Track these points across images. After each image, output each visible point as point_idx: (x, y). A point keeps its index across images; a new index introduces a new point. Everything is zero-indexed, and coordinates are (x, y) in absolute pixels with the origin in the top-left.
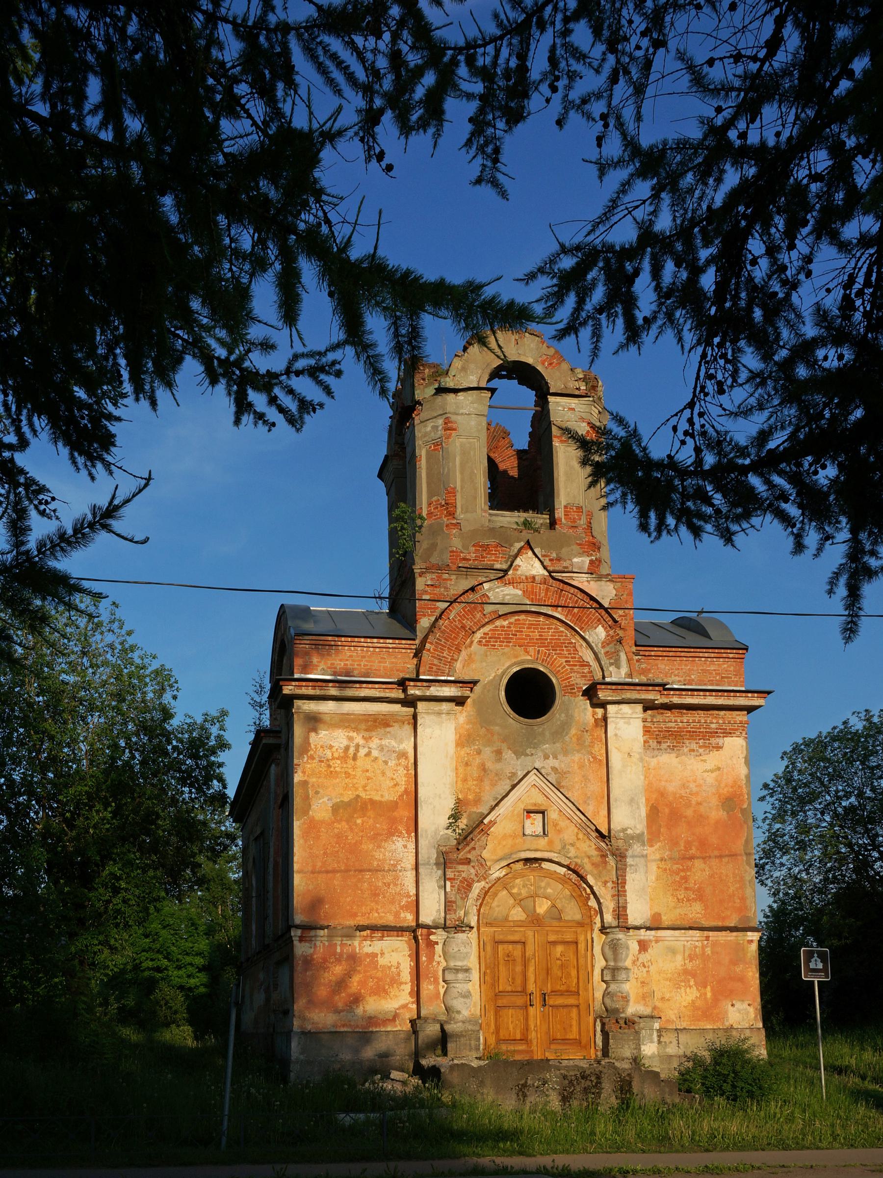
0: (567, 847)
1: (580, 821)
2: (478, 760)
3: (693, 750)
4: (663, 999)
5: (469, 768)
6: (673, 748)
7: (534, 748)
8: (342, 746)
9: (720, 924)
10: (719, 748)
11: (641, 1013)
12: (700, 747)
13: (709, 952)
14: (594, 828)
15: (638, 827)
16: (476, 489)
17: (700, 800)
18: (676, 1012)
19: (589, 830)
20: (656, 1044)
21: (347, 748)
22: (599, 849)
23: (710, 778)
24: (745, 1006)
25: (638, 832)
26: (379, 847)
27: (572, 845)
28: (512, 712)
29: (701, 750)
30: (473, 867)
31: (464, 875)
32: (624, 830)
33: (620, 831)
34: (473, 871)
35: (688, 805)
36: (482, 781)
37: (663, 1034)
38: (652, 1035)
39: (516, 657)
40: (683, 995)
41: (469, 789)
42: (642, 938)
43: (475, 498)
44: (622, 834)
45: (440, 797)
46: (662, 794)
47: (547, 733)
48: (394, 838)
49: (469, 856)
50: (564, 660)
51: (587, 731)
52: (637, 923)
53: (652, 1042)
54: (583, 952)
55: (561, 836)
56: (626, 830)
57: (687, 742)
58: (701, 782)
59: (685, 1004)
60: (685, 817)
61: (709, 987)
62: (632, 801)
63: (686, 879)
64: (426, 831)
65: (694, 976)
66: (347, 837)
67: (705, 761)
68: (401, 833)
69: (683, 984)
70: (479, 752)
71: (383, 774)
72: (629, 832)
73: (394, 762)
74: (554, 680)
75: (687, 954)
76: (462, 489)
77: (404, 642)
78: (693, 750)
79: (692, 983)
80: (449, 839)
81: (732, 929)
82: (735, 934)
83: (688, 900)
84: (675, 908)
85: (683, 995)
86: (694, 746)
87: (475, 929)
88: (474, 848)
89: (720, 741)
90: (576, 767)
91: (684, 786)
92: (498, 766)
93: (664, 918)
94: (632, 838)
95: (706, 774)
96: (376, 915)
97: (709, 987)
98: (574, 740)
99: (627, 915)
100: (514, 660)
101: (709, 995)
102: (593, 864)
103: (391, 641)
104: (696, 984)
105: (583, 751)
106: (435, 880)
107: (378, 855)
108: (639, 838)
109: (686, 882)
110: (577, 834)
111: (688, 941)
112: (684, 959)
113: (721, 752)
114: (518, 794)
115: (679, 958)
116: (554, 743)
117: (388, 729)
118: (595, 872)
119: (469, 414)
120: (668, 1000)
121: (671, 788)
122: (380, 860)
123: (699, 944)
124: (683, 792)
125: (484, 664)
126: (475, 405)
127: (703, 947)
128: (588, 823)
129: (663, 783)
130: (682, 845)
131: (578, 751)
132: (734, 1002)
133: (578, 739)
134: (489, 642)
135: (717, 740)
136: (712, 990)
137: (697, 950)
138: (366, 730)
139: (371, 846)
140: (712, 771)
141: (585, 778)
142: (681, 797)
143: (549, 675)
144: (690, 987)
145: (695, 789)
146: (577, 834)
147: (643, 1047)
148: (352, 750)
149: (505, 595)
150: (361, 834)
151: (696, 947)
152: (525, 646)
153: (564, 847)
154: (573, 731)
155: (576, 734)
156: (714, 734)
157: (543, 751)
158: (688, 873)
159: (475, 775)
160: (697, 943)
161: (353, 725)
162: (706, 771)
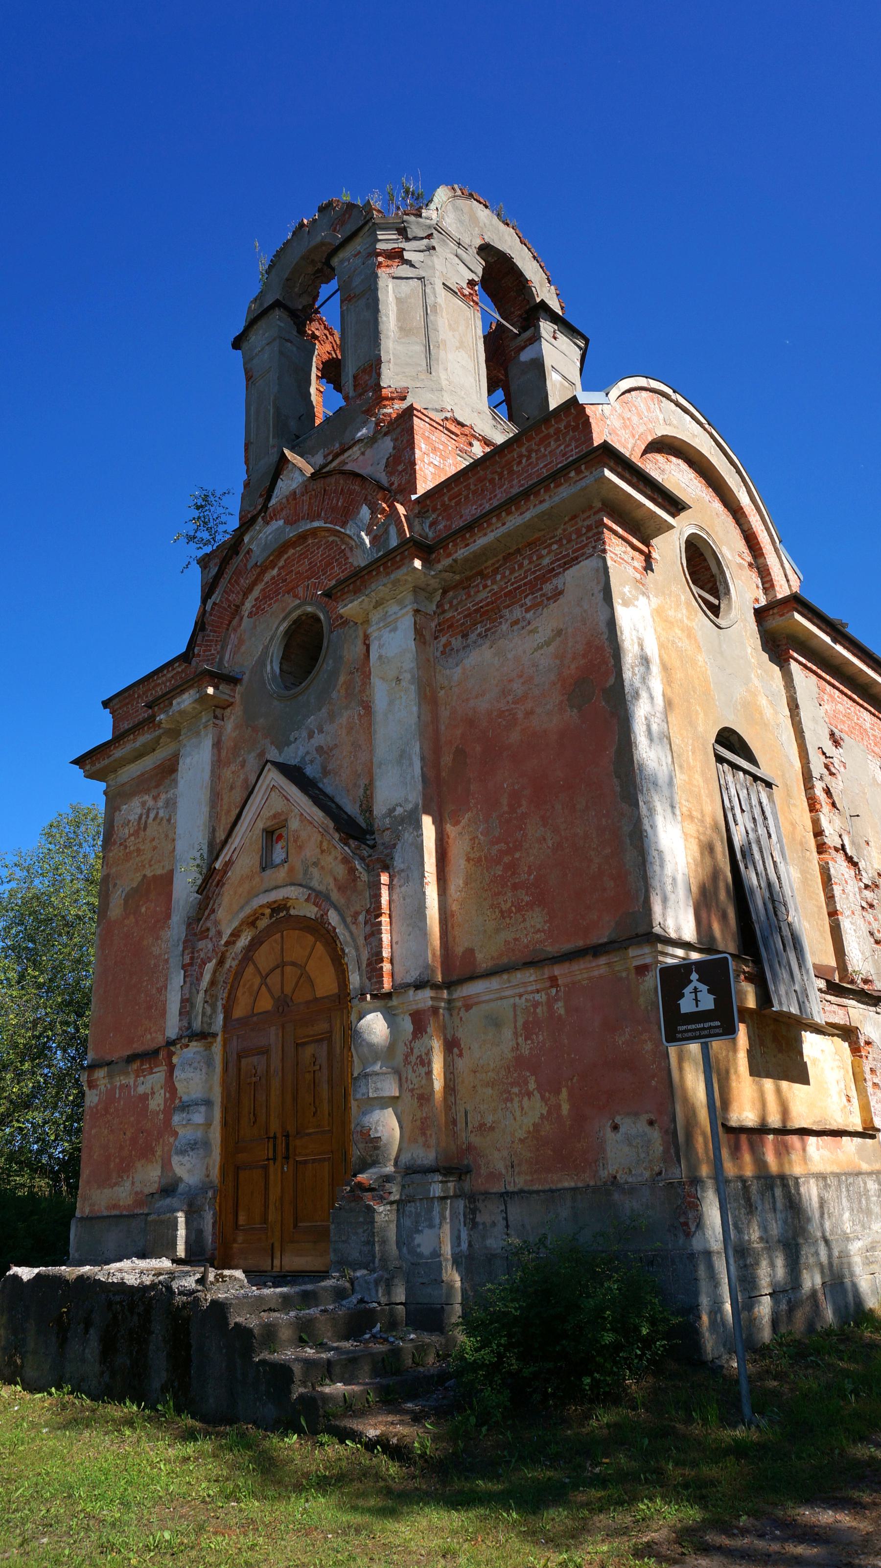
4: (482, 1126)
9: (580, 943)
10: (558, 594)
13: (562, 1011)
18: (505, 1153)
24: (641, 1126)
27: (315, 864)
29: (529, 616)
37: (480, 1205)
40: (518, 1114)
42: (414, 1007)
54: (338, 1051)
57: (506, 612)
59: (520, 1134)
61: (564, 1093)
62: (403, 756)
63: (512, 867)
69: (516, 1090)
72: (399, 811)
75: (520, 1023)
79: (532, 1086)
81: (596, 951)
82: (603, 960)
83: (519, 909)
84: (497, 931)
85: (518, 1114)
86: (518, 612)
87: (219, 1039)
89: (558, 582)
91: (504, 693)
93: (479, 956)
96: (149, 1036)
97: (564, 1093)
101: (565, 1108)
104: (539, 1088)
107: (156, 951)
109: (513, 874)
110: (321, 842)
111: (520, 996)
112: (515, 1034)
113: (562, 600)
114: (254, 809)
115: (507, 1033)
120: (492, 1129)
123: (541, 997)
132: (618, 1120)
136: (571, 1095)
137: (539, 1010)
140: (547, 644)
144: (529, 1094)
146: (321, 842)
151: (536, 1005)
156: (551, 573)
160: (537, 997)
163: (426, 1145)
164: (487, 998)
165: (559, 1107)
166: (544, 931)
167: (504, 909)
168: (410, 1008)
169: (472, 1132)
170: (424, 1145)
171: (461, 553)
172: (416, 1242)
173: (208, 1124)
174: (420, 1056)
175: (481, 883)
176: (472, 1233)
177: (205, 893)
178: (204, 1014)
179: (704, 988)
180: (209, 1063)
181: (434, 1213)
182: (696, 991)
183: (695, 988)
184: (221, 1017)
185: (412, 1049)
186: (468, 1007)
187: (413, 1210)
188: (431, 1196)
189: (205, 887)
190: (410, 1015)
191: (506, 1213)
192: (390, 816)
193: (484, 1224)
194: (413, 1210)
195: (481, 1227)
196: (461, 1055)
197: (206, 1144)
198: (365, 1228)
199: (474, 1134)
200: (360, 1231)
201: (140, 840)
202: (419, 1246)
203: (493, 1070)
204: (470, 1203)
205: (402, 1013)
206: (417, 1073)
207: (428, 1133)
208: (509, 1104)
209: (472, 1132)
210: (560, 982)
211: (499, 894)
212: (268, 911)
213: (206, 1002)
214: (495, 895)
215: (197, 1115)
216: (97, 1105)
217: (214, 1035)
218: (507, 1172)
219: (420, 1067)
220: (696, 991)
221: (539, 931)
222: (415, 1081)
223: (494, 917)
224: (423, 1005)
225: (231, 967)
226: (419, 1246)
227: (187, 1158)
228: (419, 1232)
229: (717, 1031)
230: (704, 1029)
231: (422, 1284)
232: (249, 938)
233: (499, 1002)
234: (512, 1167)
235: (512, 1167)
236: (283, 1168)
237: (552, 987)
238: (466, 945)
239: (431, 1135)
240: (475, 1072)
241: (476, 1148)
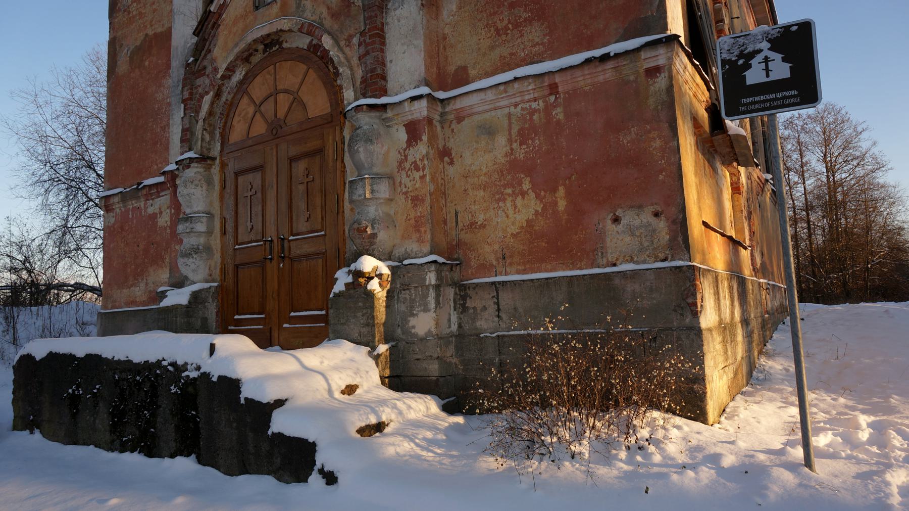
4: (473, 224)
13: (561, 116)
18: (496, 247)
20: (432, 314)
24: (646, 217)
38: (425, 296)
40: (511, 212)
42: (410, 118)
59: (514, 229)
61: (561, 191)
65: (529, 170)
69: (509, 191)
75: (515, 131)
79: (526, 186)
83: (516, 25)
84: (492, 48)
85: (511, 212)
87: (218, 161)
97: (561, 191)
101: (562, 204)
104: (535, 187)
107: (159, 96)
111: (516, 105)
112: (510, 141)
115: (501, 141)
120: (483, 226)
123: (539, 105)
127: (548, 109)
132: (619, 212)
136: (569, 194)
137: (536, 117)
144: (523, 194)
147: (413, 321)
151: (533, 112)
160: (534, 105)
163: (420, 241)
164: (480, 109)
165: (556, 203)
166: (543, 44)
167: (500, 27)
168: (405, 119)
169: (462, 230)
170: (418, 241)
172: (411, 324)
173: (209, 233)
174: (415, 162)
175: (476, 5)
176: (462, 316)
177: (201, 35)
178: (203, 140)
179: (778, 57)
180: (209, 182)
181: (429, 299)
182: (766, 60)
183: (766, 58)
184: (218, 145)
185: (406, 157)
186: (460, 120)
187: (408, 297)
188: (427, 283)
189: (201, 29)
190: (404, 125)
191: (498, 298)
193: (474, 308)
194: (408, 297)
195: (471, 311)
196: (451, 163)
197: (208, 249)
198: (364, 311)
199: (464, 231)
200: (359, 314)
201: (142, 5)
202: (413, 327)
203: (485, 174)
204: (460, 290)
205: (396, 124)
206: (411, 178)
207: (423, 230)
208: (501, 204)
209: (462, 230)
210: (560, 89)
211: (495, 13)
212: (261, 47)
213: (205, 129)
214: (491, 15)
215: (199, 224)
216: (114, 224)
217: (214, 159)
218: (499, 264)
219: (415, 172)
220: (766, 60)
221: (537, 44)
222: (409, 184)
223: (489, 35)
224: (418, 115)
225: (227, 100)
226: (413, 327)
227: (191, 260)
228: (413, 315)
229: (793, 100)
230: (776, 99)
231: (418, 359)
232: (244, 73)
233: (493, 113)
234: (504, 258)
235: (504, 258)
236: (279, 265)
237: (551, 94)
238: (459, 63)
239: (425, 231)
240: (466, 177)
241: (466, 244)
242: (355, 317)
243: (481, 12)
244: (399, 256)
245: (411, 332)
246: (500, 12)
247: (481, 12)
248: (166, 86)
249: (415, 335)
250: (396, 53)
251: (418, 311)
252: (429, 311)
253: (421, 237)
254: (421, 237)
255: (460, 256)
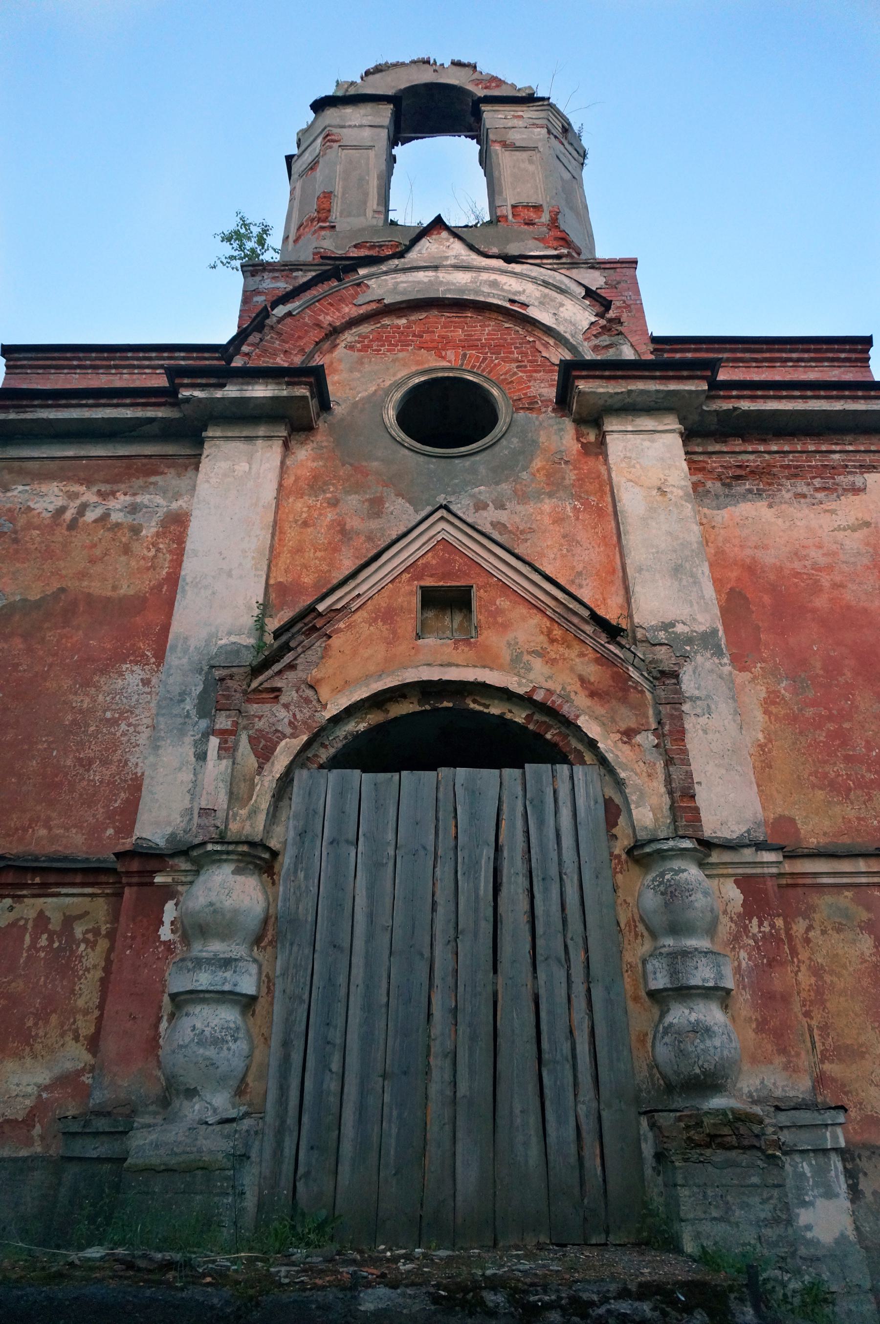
0: (526, 657)
1: (552, 603)
2: (330, 515)
3: (804, 496)
5: (309, 530)
6: (760, 493)
7: (454, 493)
8: (51, 508)
10: (857, 490)
11: (778, 1093)
12: (817, 490)
14: (586, 613)
15: (700, 618)
16: (366, 194)
17: (838, 579)
19: (576, 620)
20: (844, 1202)
21: (62, 510)
22: (604, 660)
23: (853, 542)
25: (701, 629)
26: (87, 684)
28: (408, 440)
29: (820, 495)
30: (286, 706)
31: (260, 724)
32: (667, 626)
33: (655, 629)
34: (282, 714)
35: (816, 588)
36: (336, 550)
37: (863, 1164)
39: (422, 363)
41: (305, 567)
43: (365, 203)
44: (662, 635)
45: (230, 575)
46: (751, 569)
47: (482, 470)
48: (124, 667)
49: (278, 683)
50: (514, 365)
51: (567, 462)
52: (733, 831)
53: (830, 1194)
55: (510, 636)
56: (672, 625)
58: (834, 547)
60: (814, 611)
63: (842, 737)
64: (186, 639)
66: (15, 666)
67: (833, 512)
68: (143, 655)
70: (334, 503)
71: (126, 550)
72: (680, 628)
73: (154, 530)
74: (495, 392)
76: (344, 194)
77: (206, 355)
78: (804, 496)
80: (238, 652)
86: (802, 488)
88: (291, 667)
89: (858, 480)
90: (547, 520)
92: (374, 524)
93: (804, 829)
94: (689, 640)
95: (840, 535)
96: (43, 832)
98: (541, 477)
99: (697, 810)
100: (414, 369)
102: (592, 694)
103: (182, 354)
105: (561, 494)
106: (188, 740)
108: (707, 639)
113: (862, 496)
116: (497, 483)
117: (153, 479)
118: (600, 710)
119: (361, 126)
121: (769, 558)
122: (81, 711)
124: (797, 565)
125: (357, 375)
126: (369, 118)
128: (573, 605)
129: (748, 552)
130: (818, 665)
131: (550, 495)
133: (548, 476)
134: (368, 346)
135: (850, 478)
138: (106, 482)
139: (66, 683)
141: (570, 539)
142: (797, 574)
143: (486, 385)
145: (822, 561)
147: (804, 1217)
148: (68, 515)
149: (397, 283)
150: (50, 660)
152: (438, 350)
153: (516, 659)
154: (538, 463)
155: (543, 468)
157: (473, 496)
158: (846, 725)
159: (322, 540)
161: (82, 475)
162: (839, 529)
163: (790, 1068)
170: (786, 1068)
171: (746, 405)
177: (284, 638)
192: (666, 631)
211: (825, 762)
226: (809, 1228)
228: (804, 1204)
242: (744, 1206)
243: (804, 754)
244: (749, 1092)
245: (804, 1237)
246: (832, 762)
247: (804, 754)
248: (105, 688)
249: (814, 1243)
250: (708, 775)
251: (814, 1197)
252: (837, 1196)
253: (789, 1062)
254: (789, 1062)
255: (828, 1100)
